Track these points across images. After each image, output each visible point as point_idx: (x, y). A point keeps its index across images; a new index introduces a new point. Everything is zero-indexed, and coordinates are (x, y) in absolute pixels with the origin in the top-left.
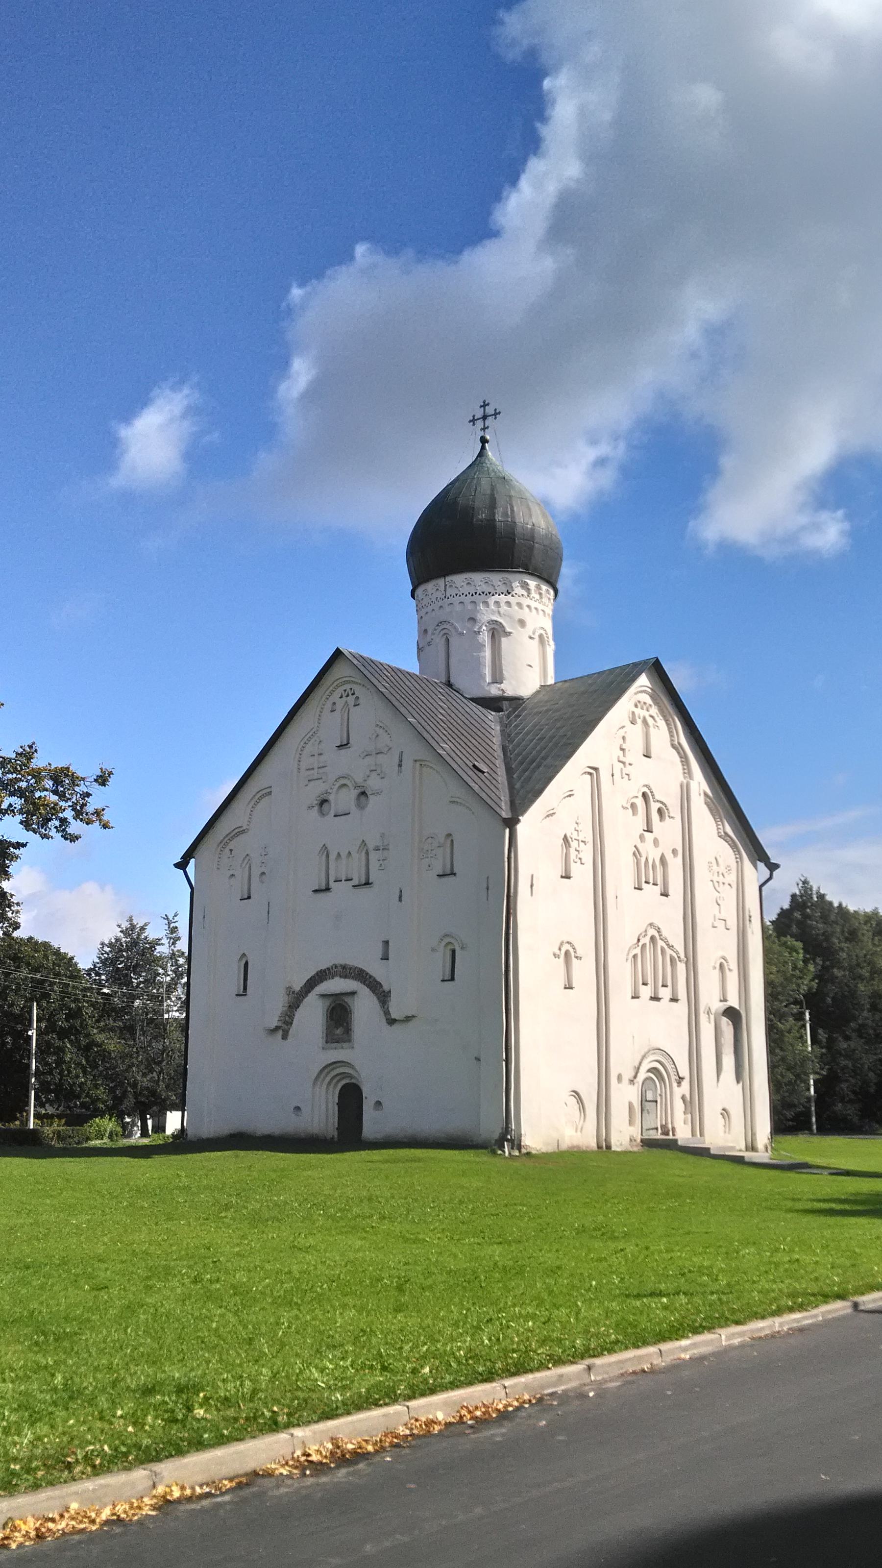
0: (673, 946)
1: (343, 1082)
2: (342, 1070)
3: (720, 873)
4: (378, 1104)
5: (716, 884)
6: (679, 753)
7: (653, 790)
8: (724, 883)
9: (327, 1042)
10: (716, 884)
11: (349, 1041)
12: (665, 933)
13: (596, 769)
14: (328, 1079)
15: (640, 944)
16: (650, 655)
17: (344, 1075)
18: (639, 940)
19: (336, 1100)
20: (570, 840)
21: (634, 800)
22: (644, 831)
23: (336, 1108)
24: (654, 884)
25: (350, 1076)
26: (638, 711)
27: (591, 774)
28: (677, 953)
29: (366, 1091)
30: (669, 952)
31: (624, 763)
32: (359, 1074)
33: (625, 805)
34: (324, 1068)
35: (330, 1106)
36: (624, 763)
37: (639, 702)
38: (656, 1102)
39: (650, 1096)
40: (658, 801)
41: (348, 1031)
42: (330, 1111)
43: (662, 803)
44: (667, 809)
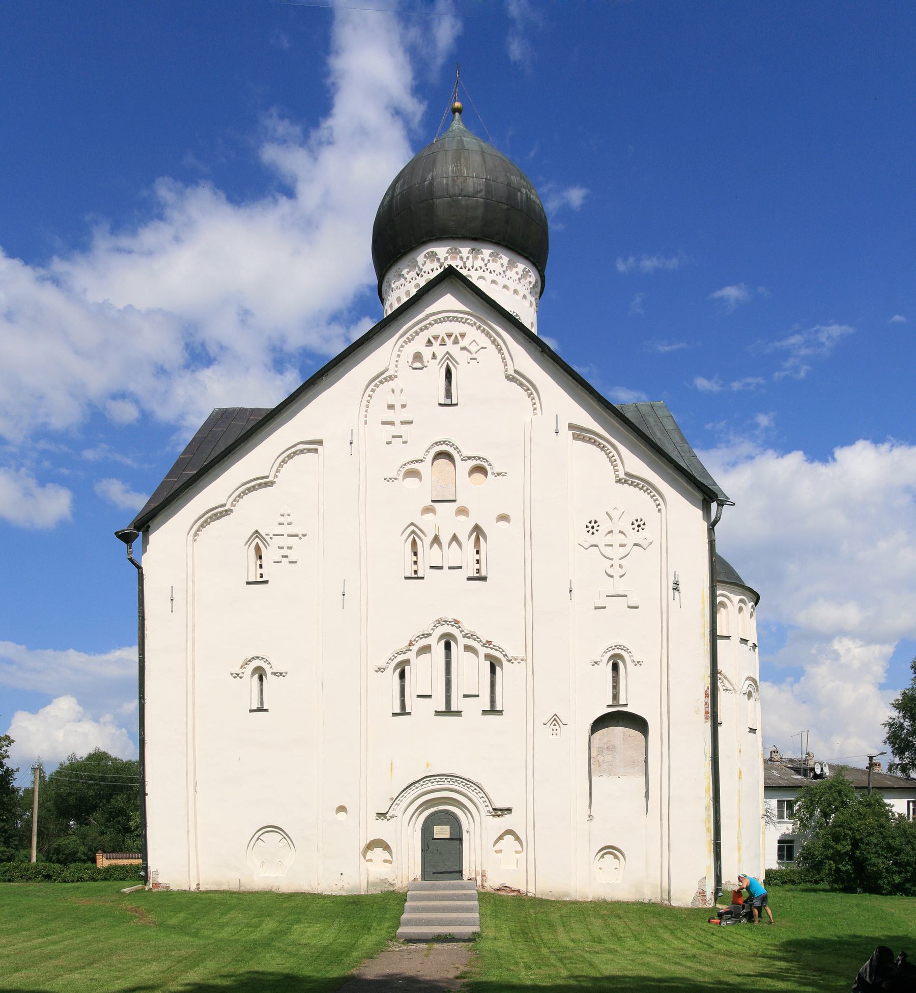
0: (489, 642)
3: (616, 531)
5: (608, 551)
6: (521, 385)
7: (458, 444)
8: (621, 545)
10: (608, 551)
12: (468, 627)
13: (320, 442)
15: (415, 649)
18: (411, 644)
20: (267, 538)
21: (413, 466)
22: (433, 501)
24: (450, 568)
26: (427, 353)
27: (316, 451)
28: (499, 649)
30: (483, 651)
31: (392, 423)
33: (389, 475)
36: (392, 423)
37: (436, 338)
38: (460, 840)
40: (469, 458)
43: (479, 458)
44: (490, 465)
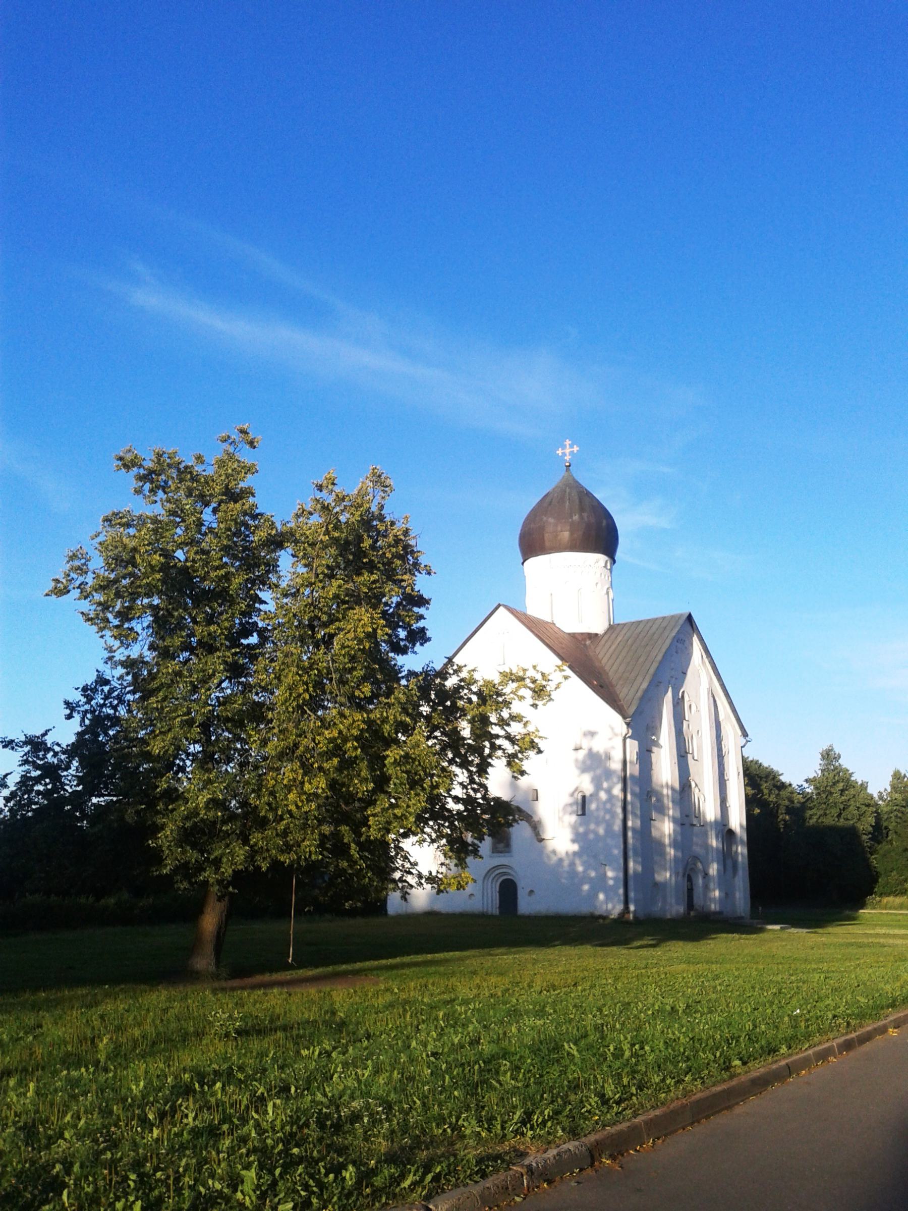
1: (505, 877)
2: (504, 870)
4: (531, 892)
9: (493, 852)
11: (509, 852)
14: (493, 875)
16: (684, 610)
17: (505, 874)
19: (498, 890)
23: (498, 894)
25: (508, 874)
29: (520, 885)
32: (516, 872)
34: (489, 871)
35: (494, 894)
39: (689, 888)
41: (508, 845)
42: (494, 898)
